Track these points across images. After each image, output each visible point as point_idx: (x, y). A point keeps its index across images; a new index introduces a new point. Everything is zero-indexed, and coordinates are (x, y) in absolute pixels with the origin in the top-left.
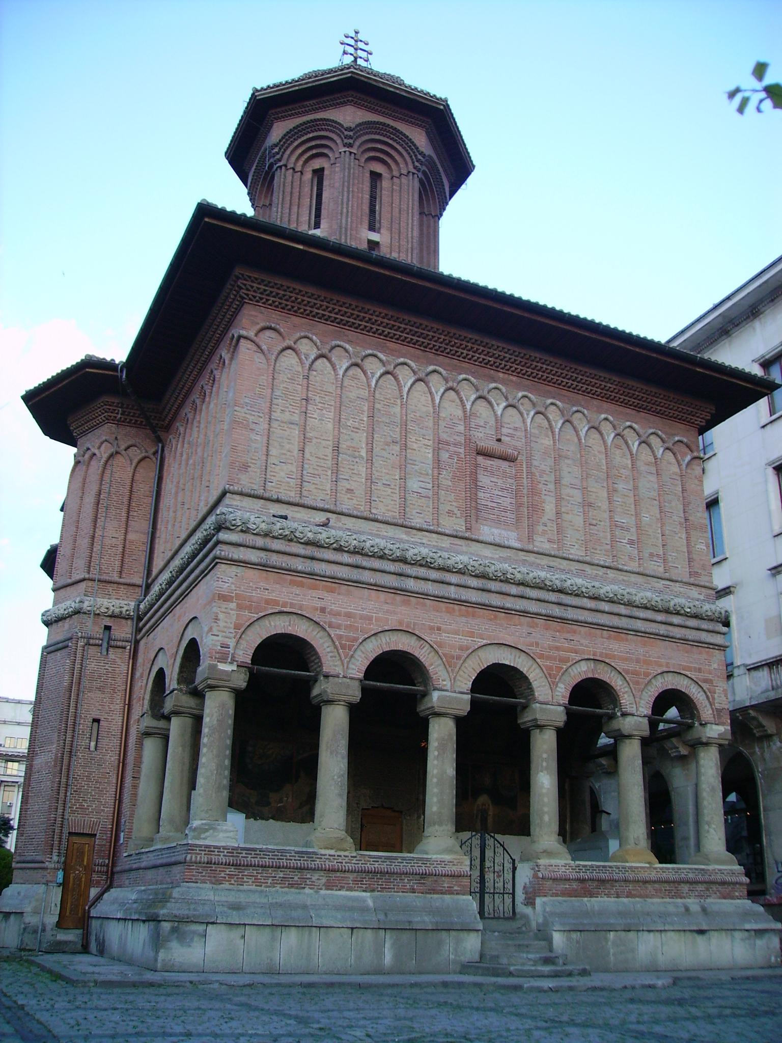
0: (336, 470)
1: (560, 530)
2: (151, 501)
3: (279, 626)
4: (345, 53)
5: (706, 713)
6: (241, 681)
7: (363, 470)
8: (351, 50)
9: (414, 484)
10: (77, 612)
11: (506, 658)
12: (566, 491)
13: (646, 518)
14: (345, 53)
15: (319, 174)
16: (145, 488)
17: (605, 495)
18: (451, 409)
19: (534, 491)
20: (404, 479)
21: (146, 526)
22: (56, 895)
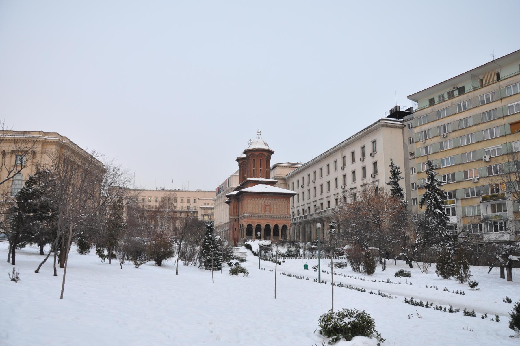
0: (253, 210)
1: (274, 212)
2: (238, 207)
3: (249, 223)
4: (257, 134)
5: (288, 226)
6: (246, 228)
7: (255, 209)
8: (258, 133)
9: (260, 210)
10: (233, 218)
11: (268, 224)
12: (274, 207)
13: (283, 209)
14: (257, 134)
15: (254, 160)
16: (238, 205)
17: (278, 207)
18: (263, 202)
19: (271, 208)
20: (259, 209)
21: (238, 209)
22: (234, 243)
